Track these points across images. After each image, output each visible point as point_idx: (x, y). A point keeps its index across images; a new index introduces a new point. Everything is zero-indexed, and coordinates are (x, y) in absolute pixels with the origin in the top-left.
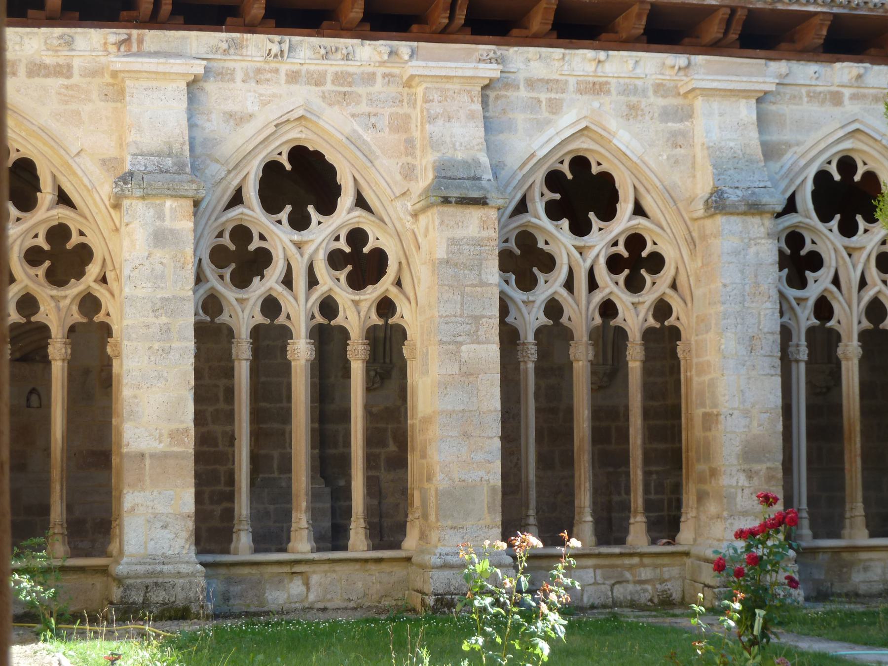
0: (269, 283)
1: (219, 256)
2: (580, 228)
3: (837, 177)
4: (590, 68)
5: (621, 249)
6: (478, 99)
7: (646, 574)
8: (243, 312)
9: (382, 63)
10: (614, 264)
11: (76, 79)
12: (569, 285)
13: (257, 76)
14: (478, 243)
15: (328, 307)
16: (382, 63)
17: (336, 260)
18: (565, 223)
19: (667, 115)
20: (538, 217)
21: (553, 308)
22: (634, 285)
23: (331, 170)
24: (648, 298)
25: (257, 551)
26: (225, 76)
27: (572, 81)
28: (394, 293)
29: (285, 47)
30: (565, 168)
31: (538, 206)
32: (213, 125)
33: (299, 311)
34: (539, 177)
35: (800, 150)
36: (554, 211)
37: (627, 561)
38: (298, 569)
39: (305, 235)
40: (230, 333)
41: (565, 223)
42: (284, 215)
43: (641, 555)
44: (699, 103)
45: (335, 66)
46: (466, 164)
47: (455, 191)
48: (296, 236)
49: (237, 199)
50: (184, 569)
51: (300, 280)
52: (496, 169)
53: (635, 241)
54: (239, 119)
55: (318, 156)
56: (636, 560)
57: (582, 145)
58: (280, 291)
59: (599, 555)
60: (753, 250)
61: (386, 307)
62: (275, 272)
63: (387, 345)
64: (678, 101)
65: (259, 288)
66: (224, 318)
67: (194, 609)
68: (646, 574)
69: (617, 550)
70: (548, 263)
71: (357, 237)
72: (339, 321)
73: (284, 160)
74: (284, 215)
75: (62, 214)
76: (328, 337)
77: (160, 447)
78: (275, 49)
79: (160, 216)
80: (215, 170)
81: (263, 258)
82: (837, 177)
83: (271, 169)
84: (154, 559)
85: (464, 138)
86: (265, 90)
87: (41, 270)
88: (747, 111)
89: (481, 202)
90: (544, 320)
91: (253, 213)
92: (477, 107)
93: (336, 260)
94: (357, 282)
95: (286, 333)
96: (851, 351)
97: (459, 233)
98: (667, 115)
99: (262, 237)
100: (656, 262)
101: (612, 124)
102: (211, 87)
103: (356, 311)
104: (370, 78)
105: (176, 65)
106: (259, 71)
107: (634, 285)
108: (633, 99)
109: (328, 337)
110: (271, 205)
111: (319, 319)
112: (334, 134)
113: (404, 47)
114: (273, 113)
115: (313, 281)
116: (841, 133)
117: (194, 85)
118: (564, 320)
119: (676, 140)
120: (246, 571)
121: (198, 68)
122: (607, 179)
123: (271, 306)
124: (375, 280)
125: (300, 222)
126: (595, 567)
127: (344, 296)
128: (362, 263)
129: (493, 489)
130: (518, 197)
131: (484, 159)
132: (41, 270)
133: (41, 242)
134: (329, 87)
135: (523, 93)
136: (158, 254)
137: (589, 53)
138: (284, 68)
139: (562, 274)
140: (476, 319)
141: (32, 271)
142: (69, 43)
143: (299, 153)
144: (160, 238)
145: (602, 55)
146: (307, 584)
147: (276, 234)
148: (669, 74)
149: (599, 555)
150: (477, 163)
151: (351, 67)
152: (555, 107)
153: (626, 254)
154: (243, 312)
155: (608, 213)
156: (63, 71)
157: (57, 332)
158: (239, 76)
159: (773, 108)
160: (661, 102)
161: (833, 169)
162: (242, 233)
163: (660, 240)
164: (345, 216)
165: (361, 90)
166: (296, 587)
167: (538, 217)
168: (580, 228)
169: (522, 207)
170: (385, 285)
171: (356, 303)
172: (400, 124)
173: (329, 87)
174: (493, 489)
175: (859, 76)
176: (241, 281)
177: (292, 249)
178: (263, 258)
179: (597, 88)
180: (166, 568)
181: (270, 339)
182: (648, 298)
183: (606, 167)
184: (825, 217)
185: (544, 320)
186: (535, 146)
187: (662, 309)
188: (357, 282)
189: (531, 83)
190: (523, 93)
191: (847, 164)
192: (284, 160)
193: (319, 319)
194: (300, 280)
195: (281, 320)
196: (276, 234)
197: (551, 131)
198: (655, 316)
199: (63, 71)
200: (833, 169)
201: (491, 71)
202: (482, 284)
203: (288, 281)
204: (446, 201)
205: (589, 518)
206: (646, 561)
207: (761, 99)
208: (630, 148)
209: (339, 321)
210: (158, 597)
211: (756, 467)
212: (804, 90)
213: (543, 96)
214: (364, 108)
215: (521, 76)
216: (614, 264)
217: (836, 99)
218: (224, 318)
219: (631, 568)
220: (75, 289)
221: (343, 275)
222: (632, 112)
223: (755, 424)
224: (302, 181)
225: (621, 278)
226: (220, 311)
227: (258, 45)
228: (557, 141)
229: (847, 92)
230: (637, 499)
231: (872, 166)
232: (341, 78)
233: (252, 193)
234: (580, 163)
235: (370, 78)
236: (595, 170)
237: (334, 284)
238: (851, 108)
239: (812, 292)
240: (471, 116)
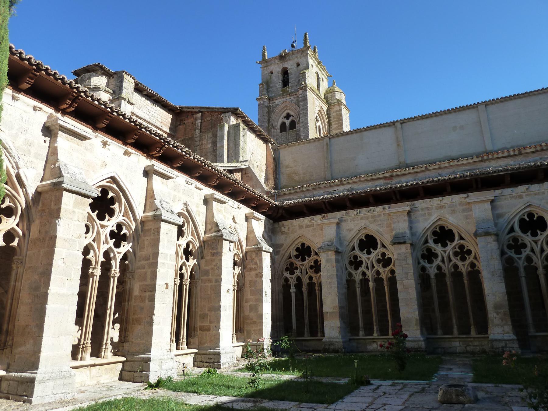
0: (363, 268)
1: (351, 263)
2: (445, 245)
3: (528, 220)
4: (439, 202)
5: (457, 249)
6: (406, 216)
7: (476, 343)
8: (357, 276)
9: (382, 212)
10: (456, 254)
11: (315, 227)
12: (443, 261)
13: (353, 219)
14: (405, 253)
15: (378, 273)
16: (382, 212)
17: (379, 261)
18: (440, 244)
19: (463, 211)
20: (431, 244)
21: (439, 268)
22: (463, 259)
23: (376, 239)
24: (467, 262)
25: (366, 335)
26: (346, 221)
27: (434, 206)
28: (393, 268)
29: (358, 212)
30: (438, 230)
31: (431, 242)
32: (344, 233)
33: (370, 274)
34: (429, 233)
35: (510, 214)
36: (436, 242)
37: (469, 340)
38: (375, 340)
39: (370, 256)
40: (354, 281)
41: (440, 244)
42: (365, 252)
43: (474, 338)
44: (473, 206)
45: (371, 213)
46: (402, 233)
47: (398, 241)
48: (444, 249)
49: (353, 249)
50: (338, 340)
51: (304, 272)
52: (413, 234)
53: (462, 247)
54: (350, 230)
55: (372, 236)
56: (472, 339)
57: (440, 223)
58: (365, 270)
59: (459, 338)
60: (489, 246)
61: (393, 272)
62: (364, 265)
63: (393, 281)
64: (467, 206)
65: (360, 270)
66: (353, 278)
67: (340, 350)
68: (476, 343)
69: (468, 336)
70: (436, 256)
71: (383, 255)
72: (381, 276)
73: (364, 238)
74: (365, 252)
75: (316, 257)
76: (378, 281)
77: (331, 311)
78: (356, 212)
79: (328, 256)
80: (346, 243)
81: (361, 262)
82: (528, 220)
83: (361, 241)
84: (331, 338)
85: (402, 226)
86: (356, 222)
87: (313, 270)
88: (488, 206)
89: (404, 243)
90: (436, 271)
91: (357, 252)
92: (406, 218)
93: (379, 261)
94: (384, 266)
95: (368, 280)
96: (541, 271)
97: (400, 252)
98: (463, 211)
99: (360, 257)
100: (469, 252)
101: (447, 216)
102: (343, 224)
103: (384, 273)
104: (380, 215)
105: (332, 221)
106: (353, 218)
107: (463, 259)
108: (453, 208)
109: (378, 281)
110: (361, 249)
111: (376, 276)
112: (374, 229)
113: (387, 206)
114: (358, 228)
115: (373, 267)
116: (524, 207)
117: (338, 224)
118: (443, 271)
119: (467, 217)
120: (362, 341)
121: (337, 220)
122: (451, 231)
123: (364, 274)
124: (389, 265)
125: (369, 253)
126: (460, 341)
127: (381, 270)
128: (386, 261)
129: (417, 320)
130: (424, 239)
131: (408, 231)
132: (313, 270)
133: (313, 264)
134: (370, 219)
135: (421, 212)
136: (328, 265)
137: (437, 199)
138: (359, 217)
139: (440, 258)
140: (407, 273)
141: (311, 271)
142: (313, 219)
143: (367, 236)
144: (328, 261)
145: (441, 198)
146: (377, 344)
147: (363, 256)
148: (463, 200)
149: (459, 338)
150: (405, 233)
151: (375, 214)
152: (430, 214)
153: (459, 251)
154: (357, 276)
155: (452, 240)
156: (312, 226)
157: (432, 276)
158: (349, 220)
159: (499, 203)
160: (462, 208)
161: (526, 217)
162: (356, 257)
163: (469, 245)
164: (380, 250)
165: (378, 219)
166: (375, 345)
167: (431, 244)
168: (445, 245)
169: (426, 242)
170: (391, 266)
171: (384, 272)
172: (389, 226)
173: (370, 219)
174: (417, 320)
175: (527, 189)
176: (356, 269)
177: (366, 260)
178: (361, 262)
179: (442, 207)
180: (334, 340)
181: (365, 281)
182: (467, 262)
183: (449, 228)
184: (524, 231)
185: (361, 277)
186: (426, 225)
187: (473, 265)
188: (384, 266)
189: (422, 209)
190: (421, 212)
191: (531, 215)
192: (364, 238)
193: (376, 276)
194: (304, 272)
195: (367, 277)
196: (363, 256)
197: (430, 221)
198: (471, 267)
199: (312, 226)
200: (526, 217)
201: (408, 208)
202: (408, 264)
203: (367, 268)
204: (394, 244)
205: (456, 327)
206: (476, 339)
207: (492, 201)
208: (453, 221)
209: (381, 276)
210: (332, 347)
211: (500, 311)
212: (508, 196)
213: (426, 212)
214: (379, 223)
215: (419, 208)
216: (456, 254)
217: (520, 197)
218: (353, 278)
219: (471, 341)
220: (388, 268)
221: (381, 265)
222: (453, 212)
223: (497, 298)
224: (369, 243)
225: (458, 258)
226: (426, 270)
227: (352, 212)
228: (432, 223)
229: (524, 194)
230: (472, 322)
231: (540, 214)
232: (373, 217)
233: (356, 247)
234: (442, 228)
235: (380, 215)
236: (446, 229)
237: (378, 267)
238: (526, 199)
239: (524, 255)
240: (405, 220)
